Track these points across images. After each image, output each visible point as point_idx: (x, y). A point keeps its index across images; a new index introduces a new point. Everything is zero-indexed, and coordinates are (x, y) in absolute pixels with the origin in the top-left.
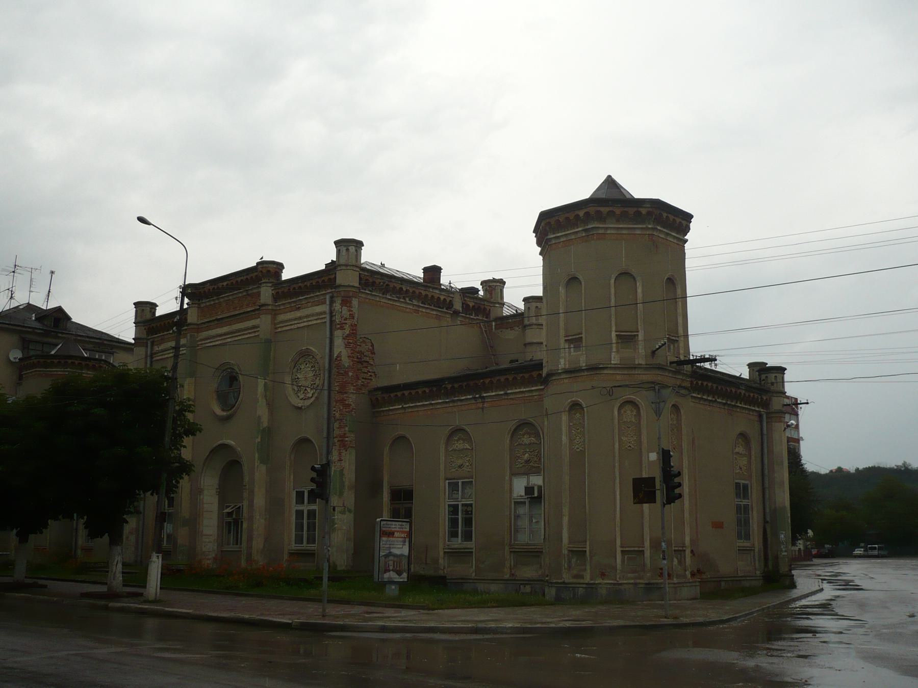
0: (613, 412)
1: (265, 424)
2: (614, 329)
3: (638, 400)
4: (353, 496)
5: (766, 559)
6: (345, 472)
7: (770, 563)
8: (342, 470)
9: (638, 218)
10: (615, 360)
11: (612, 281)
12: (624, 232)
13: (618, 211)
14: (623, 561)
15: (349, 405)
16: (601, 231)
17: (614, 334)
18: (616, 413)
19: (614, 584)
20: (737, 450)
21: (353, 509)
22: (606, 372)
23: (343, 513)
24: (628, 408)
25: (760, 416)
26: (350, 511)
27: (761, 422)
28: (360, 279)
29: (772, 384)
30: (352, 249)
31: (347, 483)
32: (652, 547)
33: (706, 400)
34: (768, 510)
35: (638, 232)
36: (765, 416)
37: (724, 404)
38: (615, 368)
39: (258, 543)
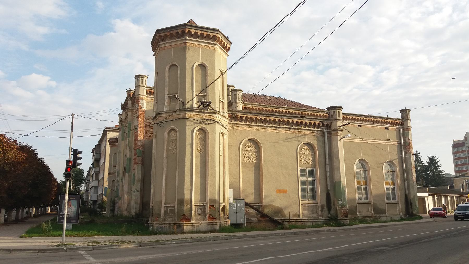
0: (164, 134)
1: (128, 157)
2: (166, 93)
3: (176, 128)
4: (140, 184)
5: (329, 209)
6: (136, 174)
7: (332, 212)
8: (134, 174)
9: (202, 36)
10: (166, 109)
11: (167, 69)
12: (173, 44)
13: (168, 34)
14: (166, 212)
15: (138, 146)
16: (163, 46)
17: (166, 96)
18: (166, 135)
19: (160, 224)
20: (303, 151)
21: (139, 190)
22: (162, 115)
23: (134, 192)
24: (173, 132)
25: (324, 133)
26: (138, 191)
27: (324, 136)
28: (147, 92)
29: (332, 116)
30: (140, 79)
31: (136, 179)
32: (178, 204)
33: (272, 127)
34: (328, 183)
35: (179, 42)
36: (326, 133)
37: (290, 128)
38: (166, 113)
39: (125, 206)
